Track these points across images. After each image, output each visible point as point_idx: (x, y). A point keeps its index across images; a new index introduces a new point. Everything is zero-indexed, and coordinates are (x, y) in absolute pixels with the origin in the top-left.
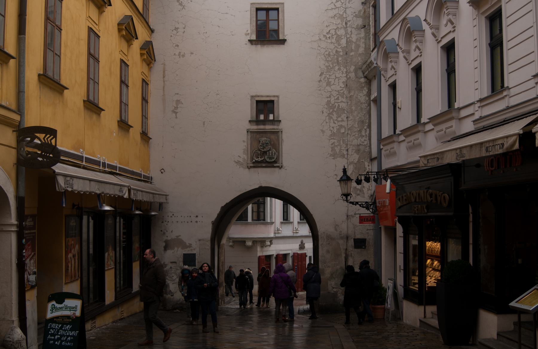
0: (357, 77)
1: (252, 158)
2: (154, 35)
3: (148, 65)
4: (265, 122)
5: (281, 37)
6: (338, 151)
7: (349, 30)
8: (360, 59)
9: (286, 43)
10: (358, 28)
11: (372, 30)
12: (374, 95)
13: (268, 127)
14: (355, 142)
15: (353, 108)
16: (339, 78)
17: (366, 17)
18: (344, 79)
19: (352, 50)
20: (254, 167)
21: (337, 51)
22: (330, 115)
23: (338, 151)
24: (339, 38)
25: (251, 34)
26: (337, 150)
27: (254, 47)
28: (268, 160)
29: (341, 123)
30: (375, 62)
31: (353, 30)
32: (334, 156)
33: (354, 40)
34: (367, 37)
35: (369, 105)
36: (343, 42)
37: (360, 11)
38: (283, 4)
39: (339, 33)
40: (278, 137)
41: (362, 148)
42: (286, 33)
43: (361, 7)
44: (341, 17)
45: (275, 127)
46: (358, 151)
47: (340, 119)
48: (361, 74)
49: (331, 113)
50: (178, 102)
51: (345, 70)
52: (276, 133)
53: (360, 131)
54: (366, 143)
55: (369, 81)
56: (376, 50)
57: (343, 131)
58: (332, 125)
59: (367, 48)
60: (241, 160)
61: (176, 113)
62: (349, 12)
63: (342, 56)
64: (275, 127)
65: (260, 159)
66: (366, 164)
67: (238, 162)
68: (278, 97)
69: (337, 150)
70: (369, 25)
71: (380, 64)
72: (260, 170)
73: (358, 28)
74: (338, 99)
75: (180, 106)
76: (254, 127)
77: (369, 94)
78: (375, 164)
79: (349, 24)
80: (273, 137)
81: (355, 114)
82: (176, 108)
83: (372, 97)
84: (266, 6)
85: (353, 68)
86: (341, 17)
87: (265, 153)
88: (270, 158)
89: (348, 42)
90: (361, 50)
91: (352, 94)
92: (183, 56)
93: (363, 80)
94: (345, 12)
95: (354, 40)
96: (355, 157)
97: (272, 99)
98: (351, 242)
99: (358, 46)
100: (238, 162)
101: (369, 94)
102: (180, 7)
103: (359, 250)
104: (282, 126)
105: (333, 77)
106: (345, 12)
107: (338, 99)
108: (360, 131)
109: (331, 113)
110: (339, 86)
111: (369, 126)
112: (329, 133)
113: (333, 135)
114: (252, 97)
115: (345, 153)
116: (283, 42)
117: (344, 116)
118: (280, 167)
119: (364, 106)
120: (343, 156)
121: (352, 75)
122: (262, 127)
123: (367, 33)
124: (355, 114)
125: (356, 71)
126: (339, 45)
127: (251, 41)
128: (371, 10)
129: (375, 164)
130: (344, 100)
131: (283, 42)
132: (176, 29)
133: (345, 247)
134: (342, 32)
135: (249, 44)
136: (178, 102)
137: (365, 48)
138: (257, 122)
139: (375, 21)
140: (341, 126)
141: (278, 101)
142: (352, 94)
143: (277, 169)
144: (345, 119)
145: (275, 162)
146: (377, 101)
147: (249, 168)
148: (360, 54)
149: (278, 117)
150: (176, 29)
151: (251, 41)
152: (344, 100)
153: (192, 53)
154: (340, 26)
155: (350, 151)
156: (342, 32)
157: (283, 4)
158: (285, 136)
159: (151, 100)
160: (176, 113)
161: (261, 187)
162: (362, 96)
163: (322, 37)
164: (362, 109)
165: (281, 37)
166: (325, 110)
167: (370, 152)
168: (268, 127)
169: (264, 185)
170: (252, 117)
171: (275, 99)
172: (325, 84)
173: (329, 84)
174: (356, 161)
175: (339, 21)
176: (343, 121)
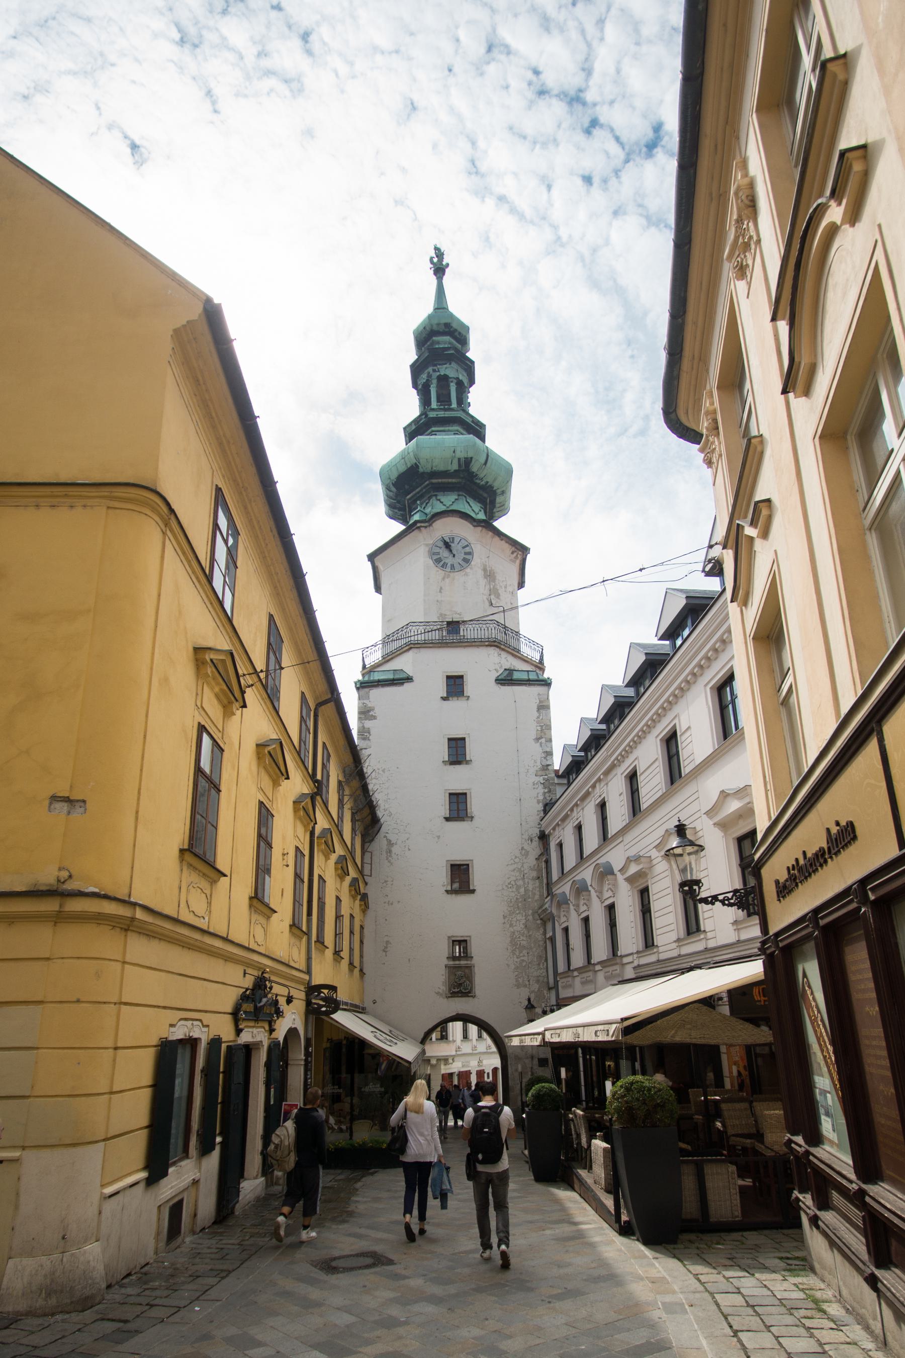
0: (534, 919)
1: (450, 990)
2: (368, 886)
3: (364, 912)
4: (459, 958)
5: (471, 888)
6: (521, 981)
7: (526, 880)
8: (536, 904)
9: (476, 893)
10: (533, 879)
11: (545, 881)
12: (549, 934)
13: (463, 962)
14: (535, 974)
15: (532, 945)
16: (519, 921)
17: (539, 870)
18: (524, 921)
19: (529, 898)
20: (452, 997)
21: (517, 899)
22: (513, 952)
23: (521, 981)
24: (518, 887)
25: (447, 885)
26: (520, 980)
27: (450, 895)
28: (463, 991)
29: (522, 958)
30: (550, 909)
31: (530, 881)
32: (518, 986)
33: (531, 889)
34: (541, 886)
35: (545, 942)
36: (522, 890)
37: (534, 866)
38: (472, 860)
39: (518, 884)
40: (471, 970)
41: (541, 979)
42: (475, 884)
43: (535, 862)
44: (520, 870)
45: (469, 962)
46: (538, 981)
47: (521, 955)
48: (537, 917)
49: (514, 950)
50: (388, 942)
51: (524, 914)
52: (470, 968)
53: (539, 964)
54: (544, 974)
55: (544, 923)
56: (549, 898)
57: (524, 964)
58: (516, 960)
59: (541, 895)
60: (441, 991)
61: (386, 952)
62: (526, 866)
63: (521, 902)
64: (469, 962)
65: (456, 990)
66: (545, 992)
67: (438, 993)
68: (470, 937)
69: (520, 980)
70: (542, 876)
71: (554, 911)
72: (456, 999)
73: (533, 879)
74: (519, 937)
75: (389, 945)
76: (452, 963)
77: (545, 933)
78: (553, 992)
79: (526, 876)
80: (467, 971)
81: (534, 949)
82: (386, 947)
83: (548, 936)
84: (458, 863)
85: (531, 912)
86: (520, 870)
87: (461, 984)
88: (465, 989)
89: (526, 890)
90: (537, 897)
91: (530, 933)
92: (392, 904)
93: (539, 922)
94: (522, 866)
95: (531, 889)
96: (536, 987)
97: (466, 938)
98: (536, 1062)
99: (535, 894)
100: (438, 993)
101: (545, 933)
102: (389, 864)
103: (543, 1068)
104: (474, 961)
105: (515, 919)
106: (522, 866)
107: (519, 937)
108: (539, 964)
109: (514, 950)
110: (519, 927)
111: (546, 960)
112: (513, 967)
113: (517, 968)
114: (449, 937)
115: (527, 983)
116: (473, 891)
117: (525, 952)
118: (474, 997)
119: (541, 943)
120: (525, 986)
121: (530, 918)
122: (457, 962)
123: (541, 883)
124: (534, 949)
125: (533, 914)
126: (519, 893)
127: (447, 891)
128: (544, 865)
129: (553, 992)
130: (525, 939)
131: (473, 891)
132: (386, 882)
133: (530, 1066)
134: (520, 883)
135: (445, 893)
136: (388, 942)
137: (540, 895)
138: (454, 958)
139: (547, 873)
140: (523, 960)
141: (470, 940)
142: (530, 933)
143: (471, 999)
144: (526, 954)
145: (469, 992)
146: (553, 940)
147: (448, 997)
148: (536, 901)
149: (471, 953)
150: (386, 882)
151: (447, 891)
152: (525, 939)
153: (399, 902)
154: (519, 878)
155: (531, 982)
156: (520, 883)
157: (472, 860)
158: (476, 970)
159: (365, 942)
160: (386, 952)
161: (457, 1014)
162: (539, 935)
163: (504, 887)
164: (539, 945)
165: (471, 888)
166: (509, 948)
167: (548, 983)
168: (463, 962)
169: (460, 1012)
170: (449, 954)
171: (468, 939)
172: (508, 926)
173: (511, 925)
174: (536, 990)
175: (518, 874)
176: (524, 956)
